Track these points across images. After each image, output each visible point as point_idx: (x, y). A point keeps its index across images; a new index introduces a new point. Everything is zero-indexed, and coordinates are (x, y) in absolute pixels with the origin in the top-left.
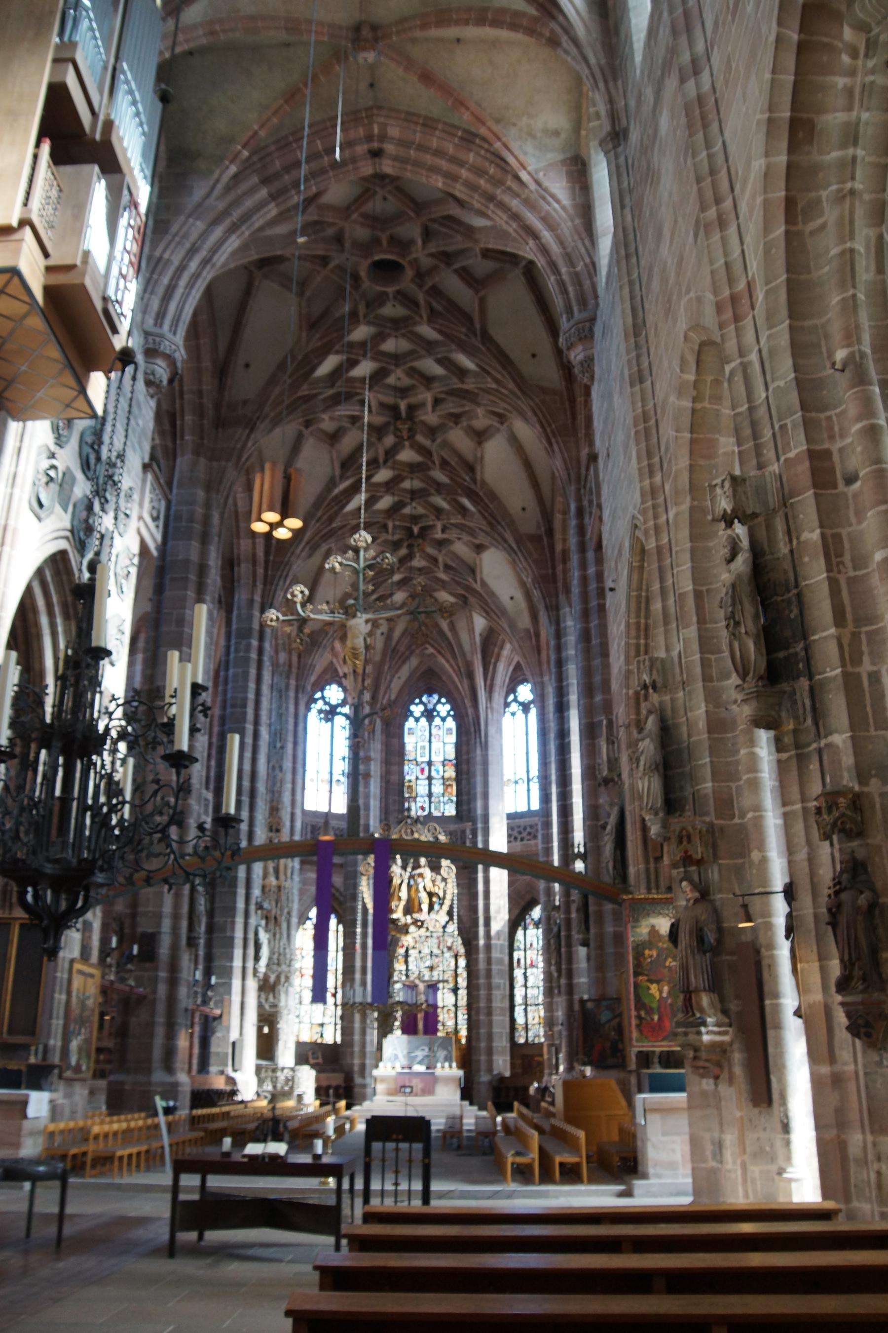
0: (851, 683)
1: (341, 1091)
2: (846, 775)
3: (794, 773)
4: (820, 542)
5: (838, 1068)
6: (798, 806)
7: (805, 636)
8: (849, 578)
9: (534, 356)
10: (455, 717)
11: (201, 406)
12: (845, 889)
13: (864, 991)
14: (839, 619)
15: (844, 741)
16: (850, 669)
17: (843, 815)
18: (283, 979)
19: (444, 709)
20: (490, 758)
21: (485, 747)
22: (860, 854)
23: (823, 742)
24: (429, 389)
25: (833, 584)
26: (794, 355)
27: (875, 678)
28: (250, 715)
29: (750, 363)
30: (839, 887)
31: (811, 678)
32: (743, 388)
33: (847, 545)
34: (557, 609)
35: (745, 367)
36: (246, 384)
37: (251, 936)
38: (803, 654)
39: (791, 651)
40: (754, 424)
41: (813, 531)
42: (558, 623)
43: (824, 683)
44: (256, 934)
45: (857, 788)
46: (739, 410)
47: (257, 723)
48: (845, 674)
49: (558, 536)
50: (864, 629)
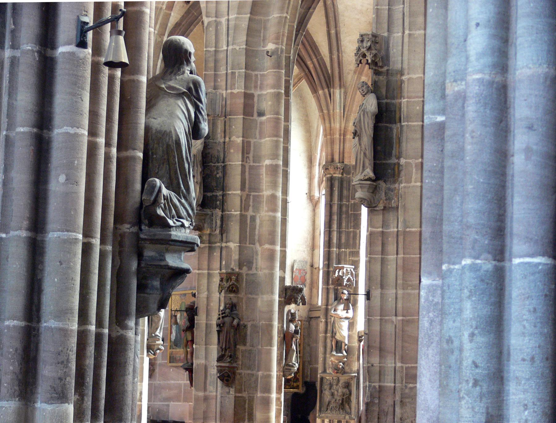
0: (243, 218)
2: (233, 263)
3: (206, 255)
4: (241, 145)
5: (207, 393)
6: (206, 271)
7: (223, 190)
8: (250, 166)
12: (227, 316)
13: (229, 362)
14: (243, 189)
15: (235, 247)
16: (243, 213)
17: (233, 284)
22: (235, 301)
23: (224, 245)
25: (243, 166)
26: (248, 35)
27: (253, 219)
29: (221, 22)
30: (223, 315)
31: (222, 212)
32: (214, 37)
33: (252, 148)
35: (218, 24)
38: (221, 197)
39: (214, 194)
40: (216, 61)
41: (238, 137)
43: (229, 216)
45: (237, 270)
46: (209, 49)
48: (241, 215)
50: (252, 194)
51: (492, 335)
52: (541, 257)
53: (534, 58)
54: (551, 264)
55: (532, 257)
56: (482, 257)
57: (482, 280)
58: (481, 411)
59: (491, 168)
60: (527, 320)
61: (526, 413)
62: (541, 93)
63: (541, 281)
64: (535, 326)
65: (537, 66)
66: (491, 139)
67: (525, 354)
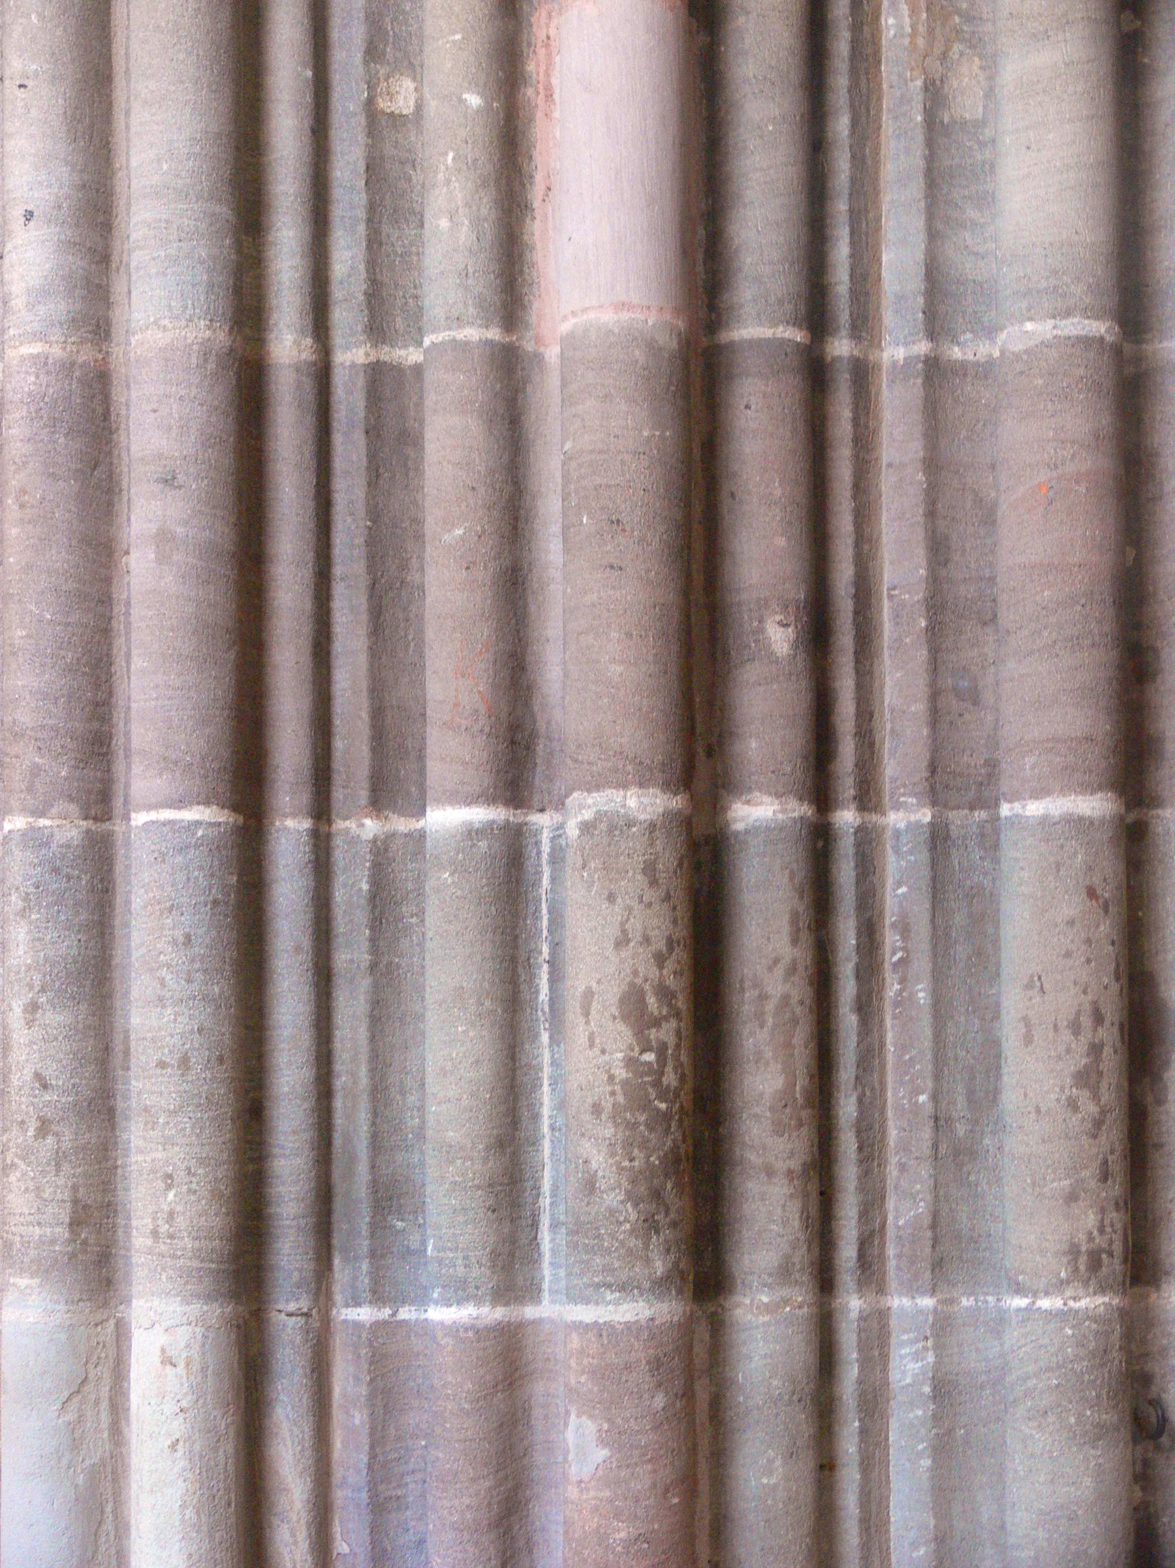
51: (83, 1007)
52: (201, 807)
53: (173, 304)
54: (227, 823)
55: (179, 808)
56: (54, 811)
57: (56, 870)
58: (59, 1196)
59: (71, 585)
60: (169, 966)
61: (171, 1195)
62: (194, 391)
63: (201, 868)
64: (189, 981)
65: (183, 323)
66: (70, 511)
67: (166, 1051)
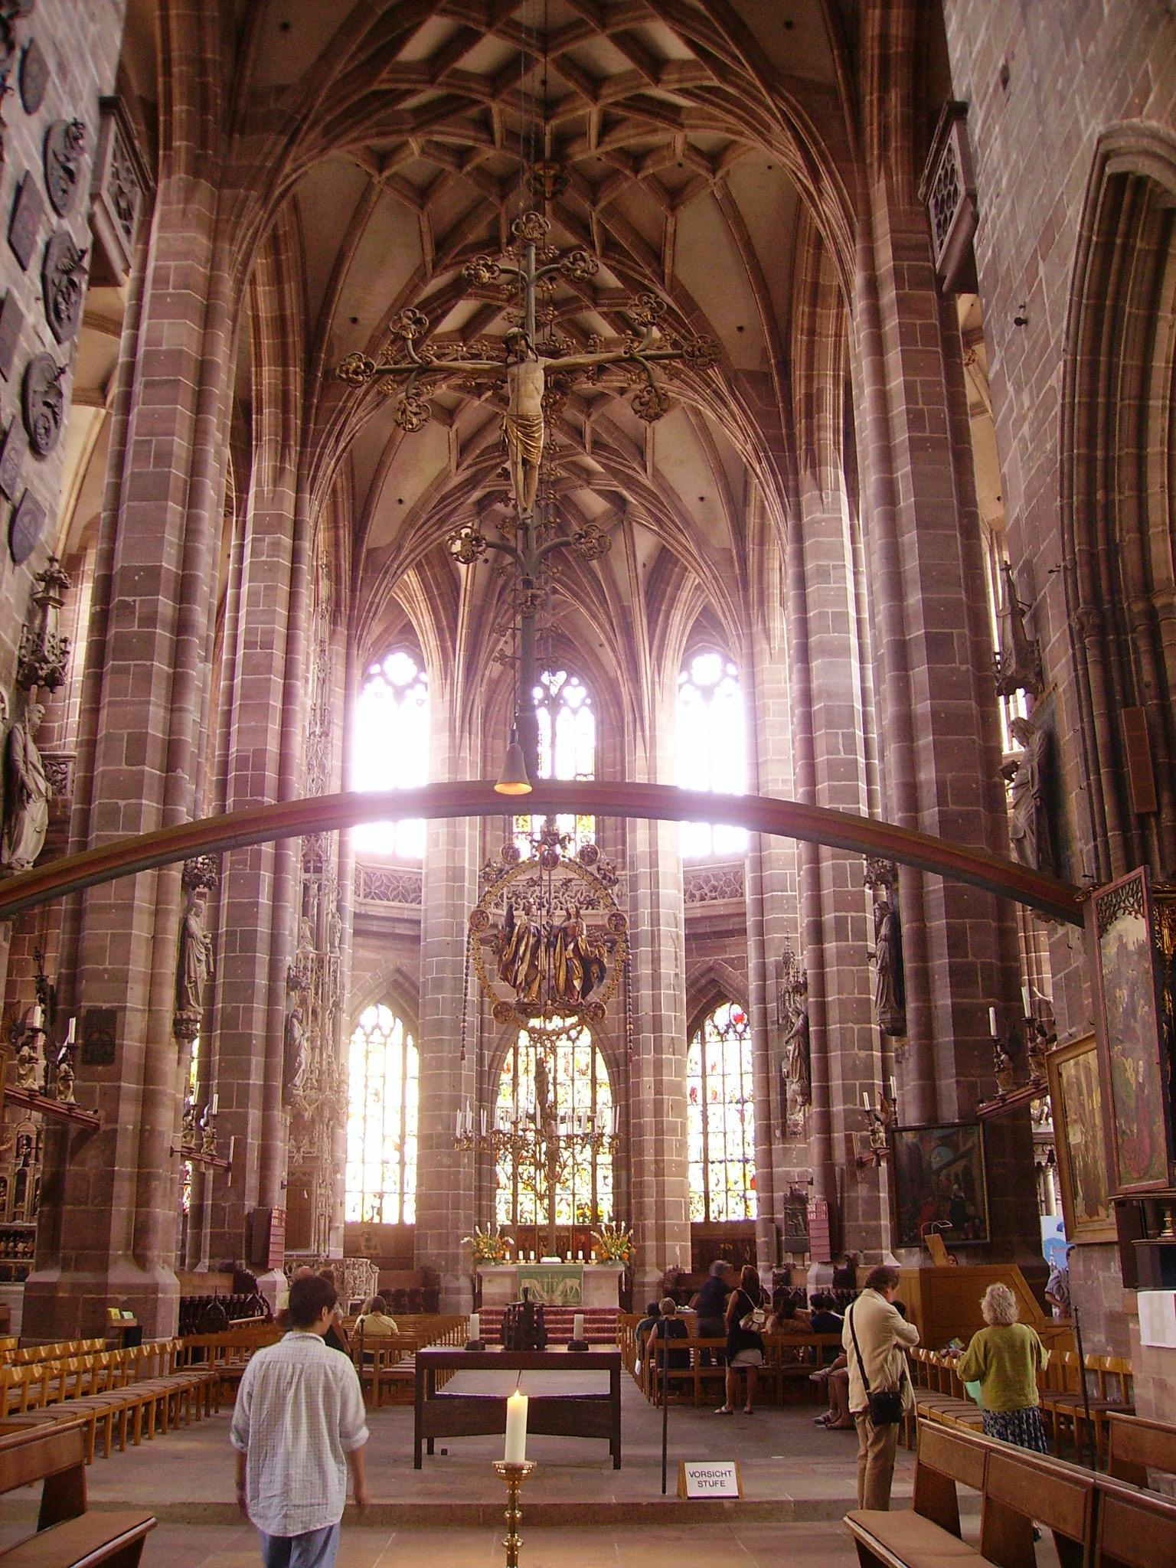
1: (419, 1300)
9: (789, 25)
10: (593, 707)
11: (204, 86)
18: (327, 1113)
19: (576, 693)
20: (659, 762)
21: (651, 745)
24: (596, 98)
28: (279, 663)
34: (797, 494)
36: (285, 59)
37: (280, 1033)
42: (798, 516)
44: (289, 1030)
47: (288, 673)
49: (799, 372)
